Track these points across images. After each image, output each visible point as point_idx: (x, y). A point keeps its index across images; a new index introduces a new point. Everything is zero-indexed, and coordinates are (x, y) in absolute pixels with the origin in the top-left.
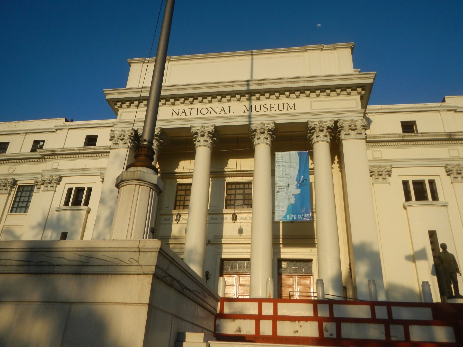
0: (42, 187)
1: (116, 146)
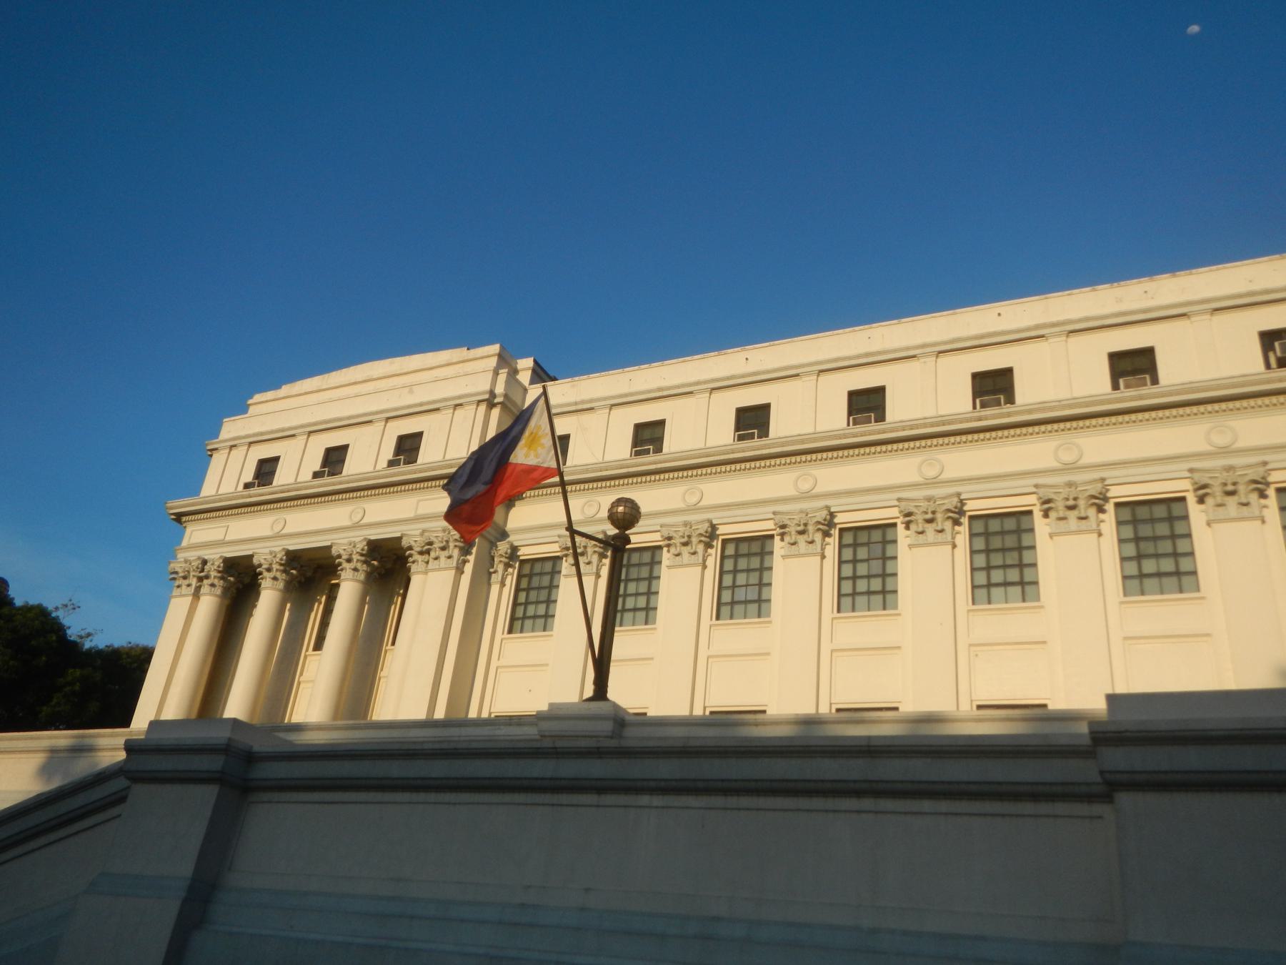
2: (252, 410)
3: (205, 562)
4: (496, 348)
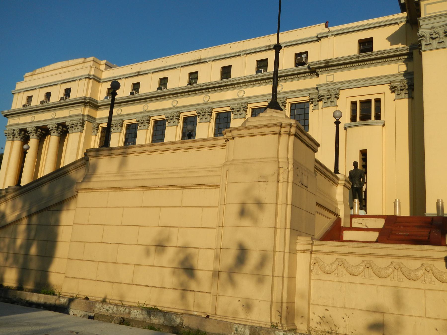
0: (321, 104)
1: (429, 47)
2: (26, 79)
3: (14, 130)
4: (92, 58)
